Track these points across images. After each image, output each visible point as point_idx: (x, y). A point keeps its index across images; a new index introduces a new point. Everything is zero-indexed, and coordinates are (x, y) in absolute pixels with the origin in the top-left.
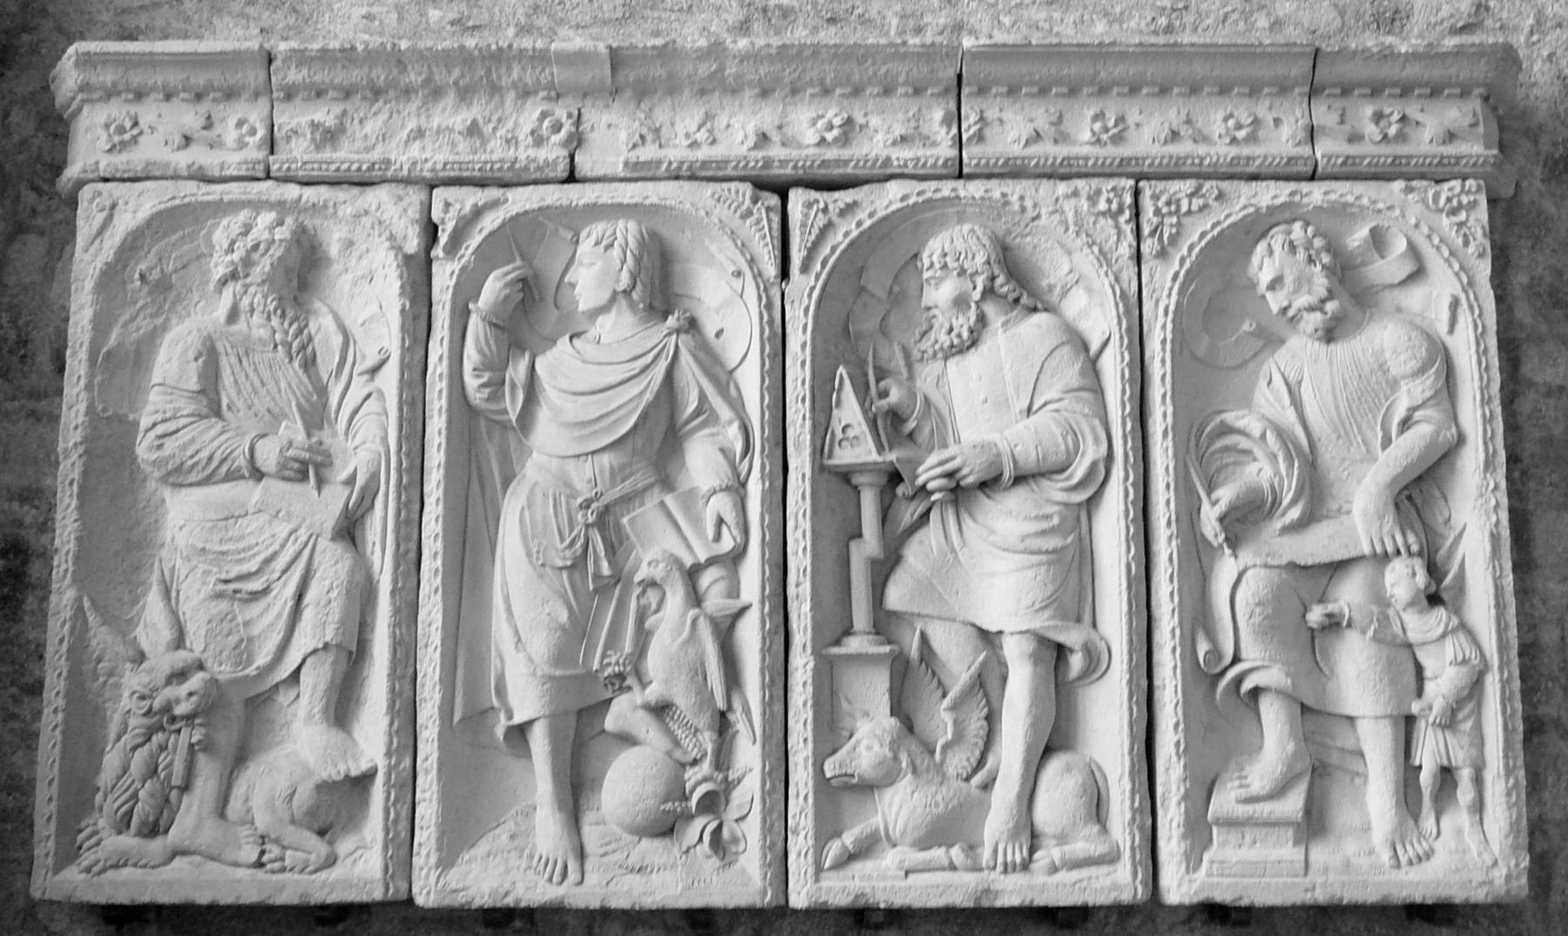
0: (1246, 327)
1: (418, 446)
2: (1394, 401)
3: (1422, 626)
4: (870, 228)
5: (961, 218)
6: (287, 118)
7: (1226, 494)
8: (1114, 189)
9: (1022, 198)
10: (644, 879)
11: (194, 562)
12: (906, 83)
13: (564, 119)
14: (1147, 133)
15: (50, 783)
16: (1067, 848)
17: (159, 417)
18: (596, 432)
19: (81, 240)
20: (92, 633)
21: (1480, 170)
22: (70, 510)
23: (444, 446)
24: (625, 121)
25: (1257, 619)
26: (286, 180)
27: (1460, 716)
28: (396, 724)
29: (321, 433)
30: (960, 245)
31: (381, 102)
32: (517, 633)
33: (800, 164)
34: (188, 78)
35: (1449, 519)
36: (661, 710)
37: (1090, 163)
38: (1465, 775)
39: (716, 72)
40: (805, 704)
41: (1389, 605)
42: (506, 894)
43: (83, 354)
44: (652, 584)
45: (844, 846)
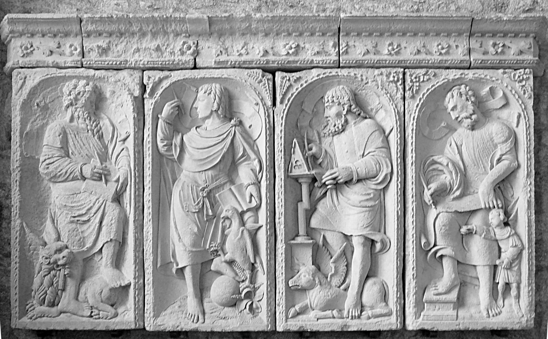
0: (443, 125)
1: (142, 168)
3: (501, 233)
4: (306, 87)
6: (89, 44)
7: (433, 186)
8: (396, 72)
9: (362, 76)
11: (62, 210)
12: (319, 31)
13: (192, 45)
14: (408, 51)
15: (16, 288)
16: (373, 311)
17: (47, 157)
18: (206, 163)
20: (27, 235)
21: (531, 65)
24: (214, 46)
25: (443, 231)
26: (89, 68)
27: (513, 265)
28: (137, 268)
30: (339, 94)
31: (123, 38)
33: (280, 62)
36: (231, 263)
37: (387, 62)
38: (514, 286)
39: (248, 26)
40: (282, 261)
41: (490, 226)
42: (178, 327)
43: (18, 134)
45: (296, 310)
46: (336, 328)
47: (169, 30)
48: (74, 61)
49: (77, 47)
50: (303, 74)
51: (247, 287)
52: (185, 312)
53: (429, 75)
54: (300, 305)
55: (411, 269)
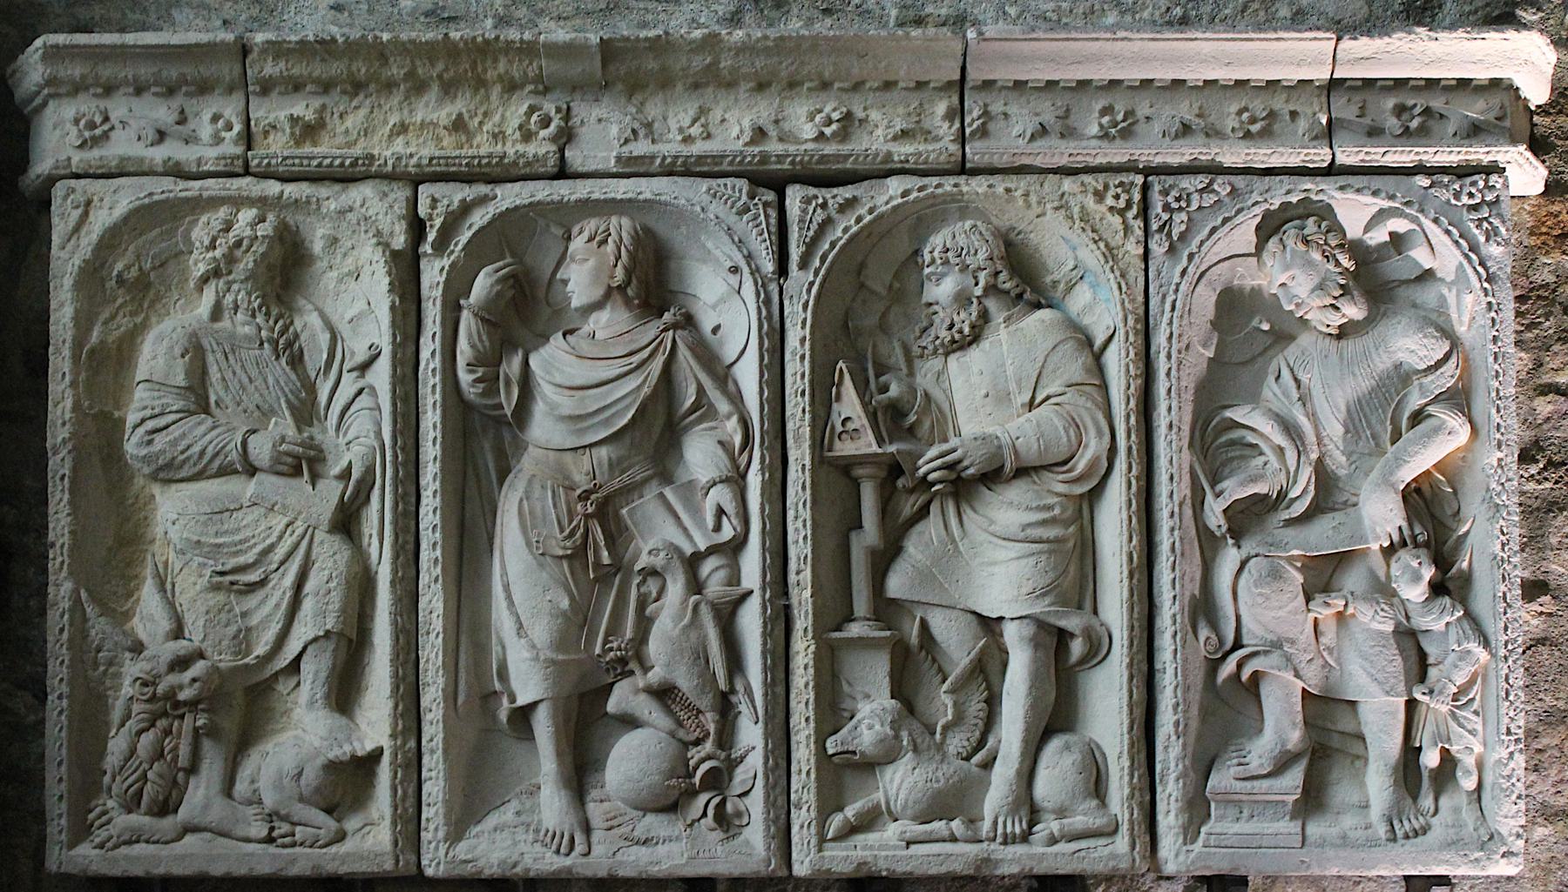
1: (412, 440)
2: (1405, 395)
6: (263, 112)
8: (1121, 184)
9: (1026, 195)
10: (650, 849)
11: (189, 556)
13: (553, 113)
15: (60, 764)
16: (1065, 821)
17: (148, 412)
18: (593, 426)
19: (56, 239)
20: (90, 623)
22: (62, 504)
24: (617, 115)
28: (400, 708)
29: (312, 429)
30: (962, 241)
31: (361, 96)
33: (798, 159)
34: (160, 71)
36: (664, 694)
39: (709, 66)
40: (806, 685)
43: (67, 352)
44: (651, 572)
47: (491, 75)
48: (225, 158)
49: (234, 120)
50: (862, 190)
51: (709, 758)
55: (1170, 708)
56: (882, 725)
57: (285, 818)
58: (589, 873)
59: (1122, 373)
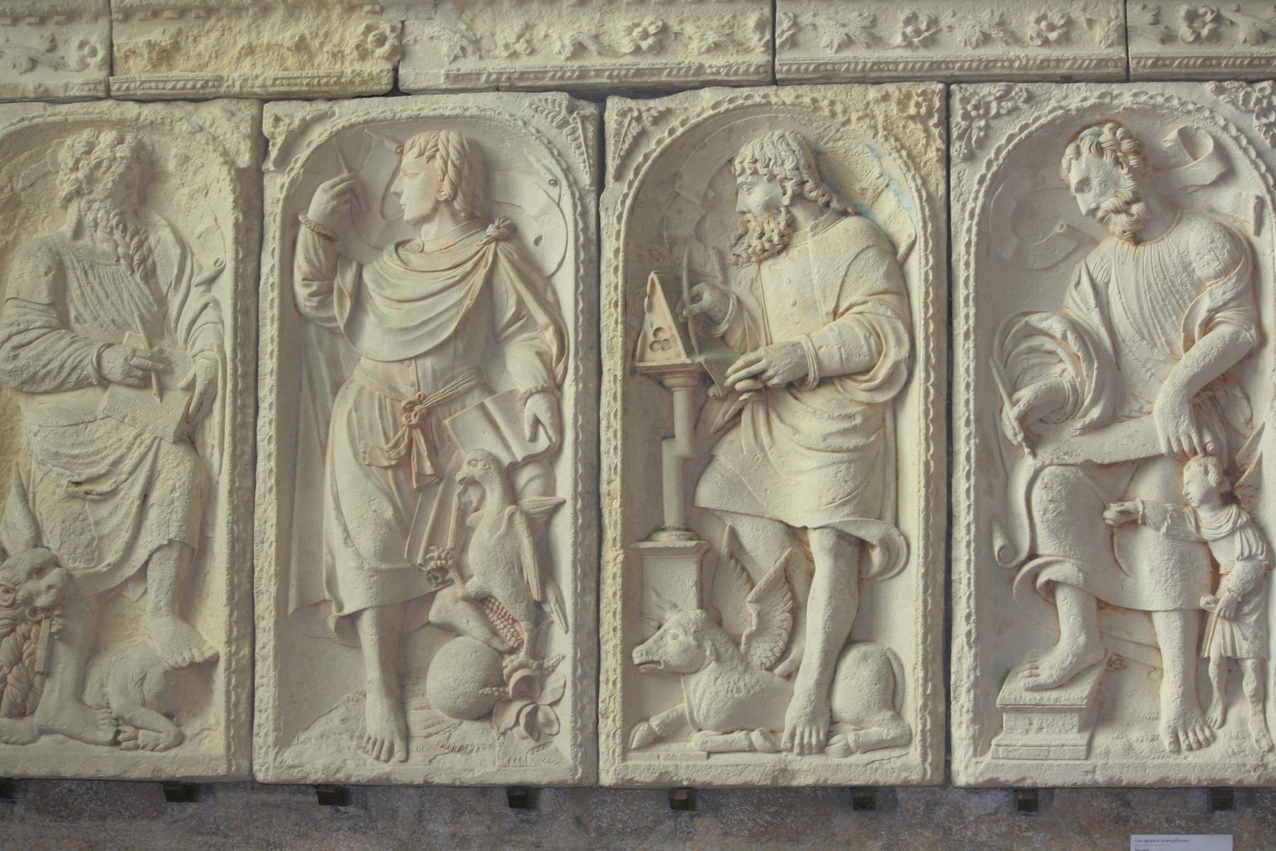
0: (1057, 229)
2: (1197, 303)
3: (1214, 523)
5: (773, 123)
7: (1026, 394)
8: (924, 93)
9: (832, 103)
13: (388, 32)
14: (959, 36)
17: (14, 329)
23: (276, 354)
25: (1050, 516)
27: (1246, 609)
28: (235, 616)
30: (770, 152)
31: (212, 21)
32: (346, 530)
33: (615, 73)
35: (1251, 419)
36: (481, 602)
37: (901, 67)
38: (1249, 665)
40: (615, 594)
42: (338, 771)
44: (471, 482)
45: (650, 728)
46: (755, 777)
48: (88, 84)
50: (677, 101)
52: (357, 734)
53: (1013, 98)
54: (663, 715)
56: (686, 634)
57: (129, 722)
58: (406, 779)
59: (922, 283)
